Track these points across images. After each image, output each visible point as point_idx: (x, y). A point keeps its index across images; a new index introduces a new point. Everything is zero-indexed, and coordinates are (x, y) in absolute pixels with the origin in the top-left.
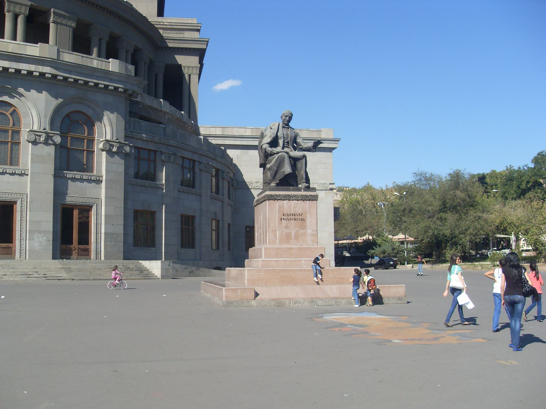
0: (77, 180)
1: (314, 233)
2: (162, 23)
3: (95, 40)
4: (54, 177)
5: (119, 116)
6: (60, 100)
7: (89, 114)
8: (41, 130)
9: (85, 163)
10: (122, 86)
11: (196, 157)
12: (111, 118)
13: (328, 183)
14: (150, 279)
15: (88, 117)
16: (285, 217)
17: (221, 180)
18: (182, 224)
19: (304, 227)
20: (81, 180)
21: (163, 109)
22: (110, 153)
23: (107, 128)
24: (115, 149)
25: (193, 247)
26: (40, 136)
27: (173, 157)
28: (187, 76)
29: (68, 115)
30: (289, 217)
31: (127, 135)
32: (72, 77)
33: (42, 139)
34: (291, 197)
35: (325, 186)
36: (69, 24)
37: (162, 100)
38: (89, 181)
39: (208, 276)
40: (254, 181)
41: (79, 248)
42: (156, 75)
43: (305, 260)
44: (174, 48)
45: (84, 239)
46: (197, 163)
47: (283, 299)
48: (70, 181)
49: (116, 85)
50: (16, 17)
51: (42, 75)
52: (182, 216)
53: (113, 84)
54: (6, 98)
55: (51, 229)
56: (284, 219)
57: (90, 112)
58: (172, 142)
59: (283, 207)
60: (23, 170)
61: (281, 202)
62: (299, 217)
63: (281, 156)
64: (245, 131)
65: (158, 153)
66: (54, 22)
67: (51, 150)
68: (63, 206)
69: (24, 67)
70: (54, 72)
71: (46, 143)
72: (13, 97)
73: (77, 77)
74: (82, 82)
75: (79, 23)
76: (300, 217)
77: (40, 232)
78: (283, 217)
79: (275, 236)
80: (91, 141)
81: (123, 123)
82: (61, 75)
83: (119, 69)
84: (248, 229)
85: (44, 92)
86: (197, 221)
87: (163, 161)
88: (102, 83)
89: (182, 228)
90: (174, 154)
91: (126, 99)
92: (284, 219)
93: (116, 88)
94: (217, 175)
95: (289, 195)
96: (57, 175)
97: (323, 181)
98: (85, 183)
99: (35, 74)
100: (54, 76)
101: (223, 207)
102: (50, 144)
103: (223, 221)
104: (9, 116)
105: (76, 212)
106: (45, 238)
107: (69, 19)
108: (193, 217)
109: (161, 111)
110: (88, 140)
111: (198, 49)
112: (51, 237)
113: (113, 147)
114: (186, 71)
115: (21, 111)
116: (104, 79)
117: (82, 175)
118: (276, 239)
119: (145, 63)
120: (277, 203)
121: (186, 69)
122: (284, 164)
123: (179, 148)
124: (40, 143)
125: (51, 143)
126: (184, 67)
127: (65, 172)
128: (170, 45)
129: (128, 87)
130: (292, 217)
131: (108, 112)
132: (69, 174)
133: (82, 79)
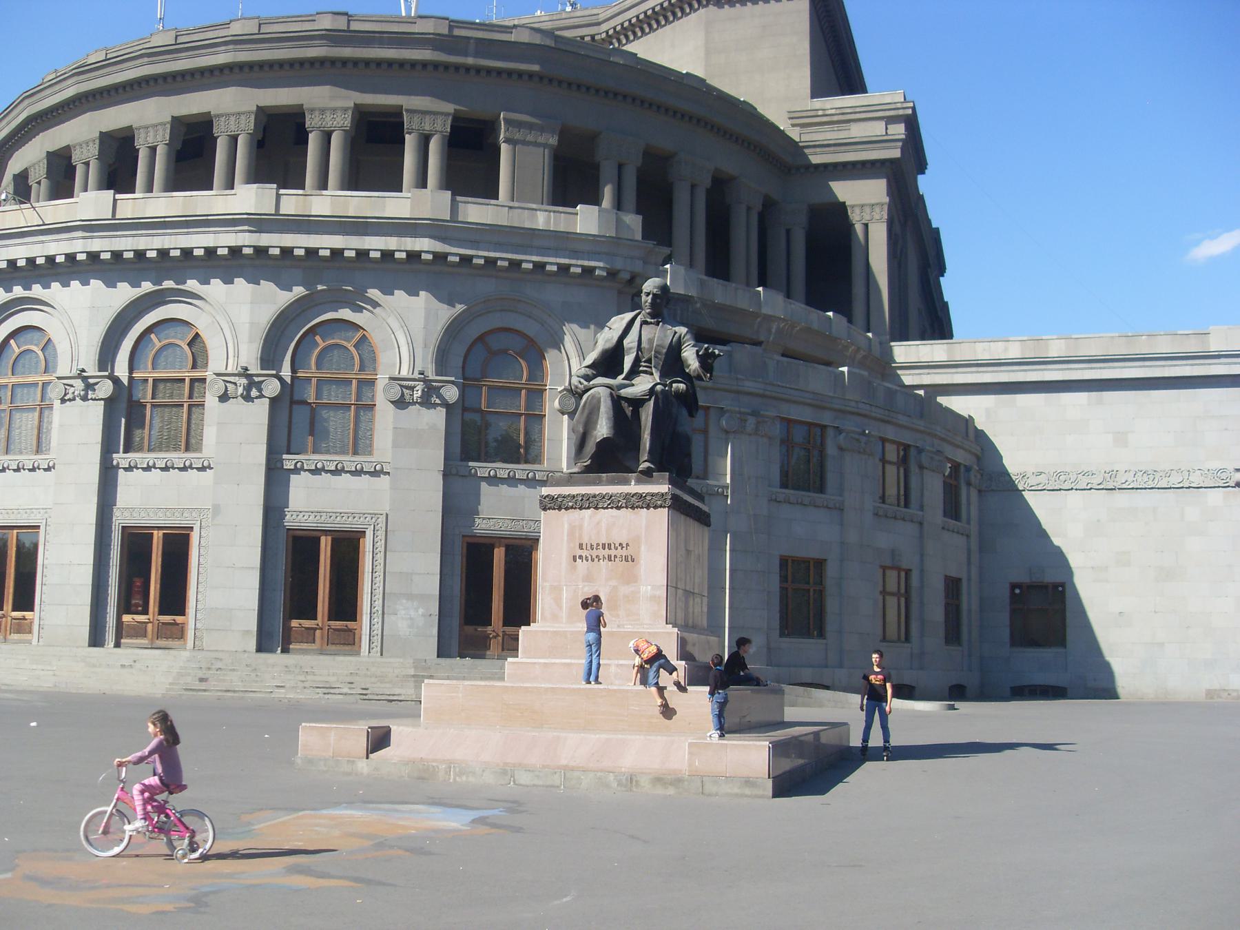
0: (502, 481)
1: (658, 593)
2: (820, 113)
3: (608, 170)
4: (444, 475)
6: (460, 308)
7: (531, 333)
8: (416, 375)
9: (522, 442)
10: (601, 264)
11: (826, 419)
12: (581, 339)
13: (1231, 467)
15: (531, 341)
17: (914, 468)
18: (784, 579)
19: (631, 579)
20: (511, 481)
21: (766, 310)
25: (821, 634)
26: (412, 388)
27: (751, 421)
28: (859, 228)
29: (481, 339)
30: (594, 553)
32: (480, 255)
33: (417, 394)
35: (1224, 476)
36: (541, 140)
37: (760, 289)
39: (804, 705)
40: (1030, 470)
42: (788, 231)
43: (618, 666)
44: (825, 166)
46: (830, 433)
47: (434, 761)
48: (484, 485)
49: (586, 263)
50: (425, 140)
51: (413, 256)
52: (784, 562)
53: (580, 262)
54: (345, 314)
55: (436, 591)
56: (581, 557)
57: (531, 328)
58: (750, 385)
59: (581, 527)
60: (379, 463)
61: (575, 515)
62: (619, 552)
63: (593, 396)
64: (1006, 349)
65: (712, 412)
66: (507, 141)
67: (438, 417)
68: (470, 540)
69: (375, 244)
71: (426, 402)
72: (359, 309)
73: (492, 254)
74: (506, 264)
75: (564, 134)
76: (624, 552)
77: (410, 597)
78: (579, 552)
79: (558, 601)
80: (537, 394)
82: (455, 252)
84: (1017, 591)
85: (422, 293)
86: (831, 571)
87: (727, 432)
88: (553, 263)
89: (784, 591)
90: (755, 413)
91: (620, 292)
92: (581, 557)
93: (588, 271)
94: (904, 461)
95: (594, 496)
96: (454, 471)
97: (1215, 465)
98: (522, 487)
99: (397, 255)
100: (440, 257)
101: (921, 537)
102: (435, 406)
103: (922, 571)
104: (352, 349)
105: (499, 555)
106: (421, 611)
107: (542, 130)
108: (820, 564)
109: (755, 315)
110: (529, 390)
111: (883, 162)
114: (855, 217)
115: (375, 336)
117: (512, 470)
118: (561, 608)
119: (749, 209)
120: (566, 519)
121: (857, 211)
123: (771, 397)
124: (414, 403)
125: (438, 401)
126: (853, 206)
127: (471, 464)
128: (815, 160)
129: (619, 264)
130: (601, 553)
131: (575, 327)
132: (483, 469)
133: (503, 257)
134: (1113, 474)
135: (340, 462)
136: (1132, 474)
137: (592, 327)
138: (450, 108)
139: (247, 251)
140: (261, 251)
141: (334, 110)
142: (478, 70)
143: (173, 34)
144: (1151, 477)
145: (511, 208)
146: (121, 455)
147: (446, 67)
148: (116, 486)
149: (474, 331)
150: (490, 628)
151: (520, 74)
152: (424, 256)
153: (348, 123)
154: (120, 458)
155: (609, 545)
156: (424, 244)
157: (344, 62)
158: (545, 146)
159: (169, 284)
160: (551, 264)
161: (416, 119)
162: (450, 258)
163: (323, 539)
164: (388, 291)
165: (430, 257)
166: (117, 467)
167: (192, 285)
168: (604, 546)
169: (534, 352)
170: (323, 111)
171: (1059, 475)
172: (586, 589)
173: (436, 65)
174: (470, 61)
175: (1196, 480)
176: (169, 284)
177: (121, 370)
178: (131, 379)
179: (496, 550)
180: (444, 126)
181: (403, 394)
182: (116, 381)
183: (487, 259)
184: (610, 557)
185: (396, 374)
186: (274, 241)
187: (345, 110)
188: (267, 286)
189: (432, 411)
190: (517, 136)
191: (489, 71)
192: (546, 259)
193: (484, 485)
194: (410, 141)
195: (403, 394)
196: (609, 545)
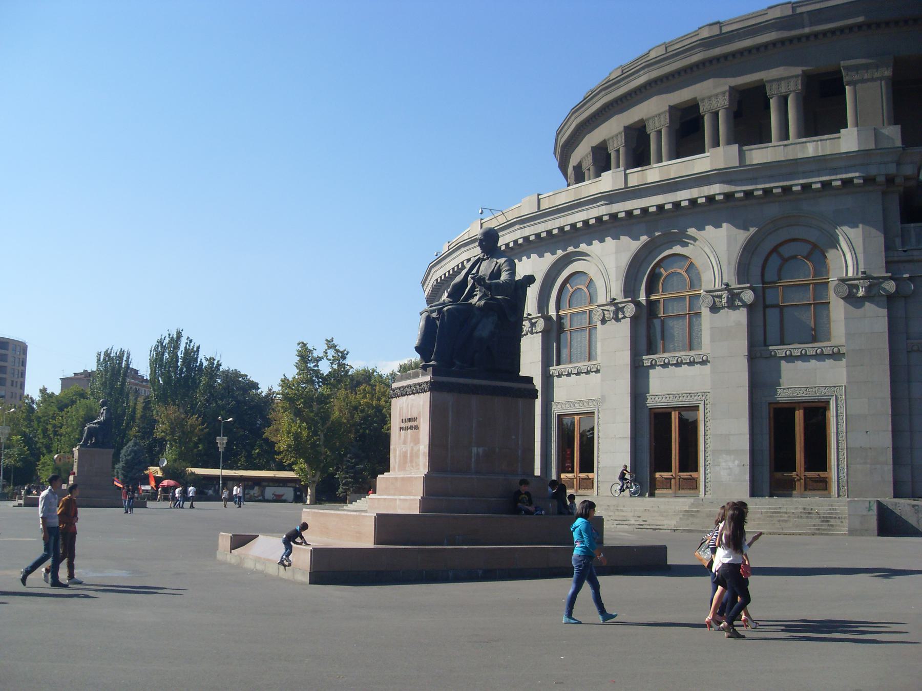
0: (798, 358)
5: (867, 227)
6: (753, 230)
7: (813, 240)
10: (857, 174)
14: (832, 534)
15: (815, 246)
16: (403, 425)
19: (416, 441)
20: (804, 357)
22: (851, 299)
23: (852, 253)
24: (861, 293)
26: (720, 297)
29: (775, 250)
31: (896, 259)
32: (758, 188)
33: (724, 301)
36: (877, 75)
38: (820, 357)
41: (806, 478)
45: (818, 458)
48: (783, 363)
50: (784, 100)
51: (710, 199)
53: (839, 177)
54: (677, 249)
60: (705, 355)
67: (741, 316)
68: (775, 406)
70: (727, 188)
71: (731, 305)
72: (686, 245)
73: (767, 186)
74: (779, 190)
77: (729, 452)
81: (879, 239)
82: (738, 190)
83: (859, 144)
85: (724, 225)
88: (816, 182)
93: (847, 183)
96: (759, 355)
98: (813, 362)
99: (700, 201)
100: (729, 196)
102: (738, 307)
104: (684, 274)
105: (799, 415)
106: (737, 462)
107: (877, 67)
112: (746, 459)
113: (858, 289)
115: (698, 262)
116: (792, 176)
117: (803, 348)
124: (723, 308)
125: (740, 304)
127: (771, 348)
129: (873, 171)
131: (846, 229)
132: (780, 350)
133: (776, 186)
135: (679, 357)
137: (861, 226)
138: (798, 70)
139: (606, 218)
140: (614, 216)
141: (717, 95)
142: (816, 35)
143: (620, 70)
145: (785, 145)
146: (555, 367)
147: (791, 40)
148: (553, 388)
149: (768, 246)
150: (794, 473)
151: (850, 28)
152: (717, 198)
153: (727, 102)
154: (554, 369)
156: (716, 189)
157: (717, 59)
158: (881, 79)
159: (571, 249)
160: (797, 185)
161: (775, 86)
162: (737, 195)
163: (673, 413)
164: (701, 228)
165: (721, 197)
166: (552, 376)
167: (583, 247)
169: (817, 253)
170: (710, 98)
173: (783, 42)
174: (807, 30)
176: (571, 249)
177: (552, 312)
178: (558, 315)
179: (797, 412)
180: (796, 86)
181: (714, 302)
182: (548, 319)
183: (764, 190)
185: (712, 288)
186: (620, 208)
187: (723, 93)
188: (625, 239)
189: (737, 311)
190: (856, 77)
191: (824, 33)
192: (810, 180)
193: (783, 363)
194: (773, 103)
195: (714, 302)
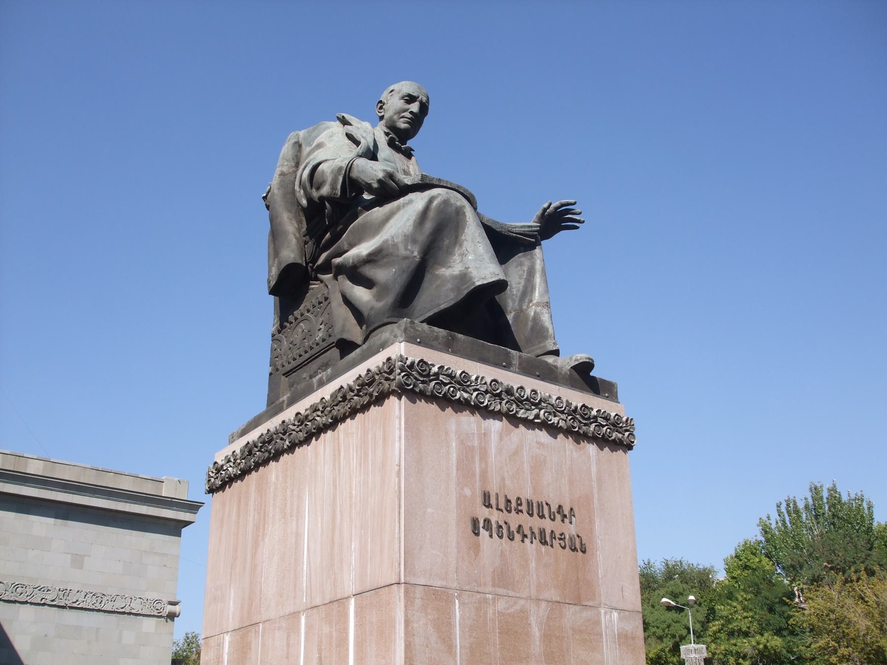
13: (165, 600)
16: (495, 517)
30: (515, 520)
34: (519, 402)
35: (158, 606)
62: (557, 526)
78: (483, 513)
79: (443, 626)
95: (509, 391)
97: (152, 595)
118: (450, 648)
122: (456, 240)
134: (65, 592)
136: (83, 594)
144: (99, 600)
155: (540, 506)
168: (530, 504)
171: (16, 586)
172: (501, 605)
175: (136, 607)
184: (542, 532)
196: (540, 506)
